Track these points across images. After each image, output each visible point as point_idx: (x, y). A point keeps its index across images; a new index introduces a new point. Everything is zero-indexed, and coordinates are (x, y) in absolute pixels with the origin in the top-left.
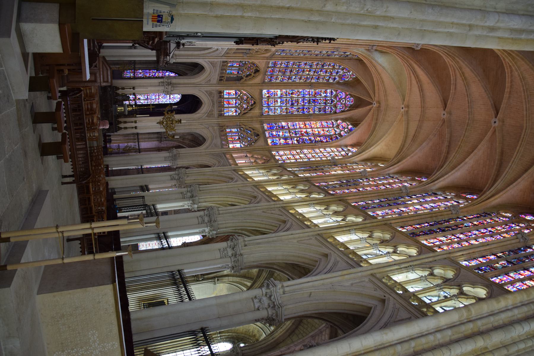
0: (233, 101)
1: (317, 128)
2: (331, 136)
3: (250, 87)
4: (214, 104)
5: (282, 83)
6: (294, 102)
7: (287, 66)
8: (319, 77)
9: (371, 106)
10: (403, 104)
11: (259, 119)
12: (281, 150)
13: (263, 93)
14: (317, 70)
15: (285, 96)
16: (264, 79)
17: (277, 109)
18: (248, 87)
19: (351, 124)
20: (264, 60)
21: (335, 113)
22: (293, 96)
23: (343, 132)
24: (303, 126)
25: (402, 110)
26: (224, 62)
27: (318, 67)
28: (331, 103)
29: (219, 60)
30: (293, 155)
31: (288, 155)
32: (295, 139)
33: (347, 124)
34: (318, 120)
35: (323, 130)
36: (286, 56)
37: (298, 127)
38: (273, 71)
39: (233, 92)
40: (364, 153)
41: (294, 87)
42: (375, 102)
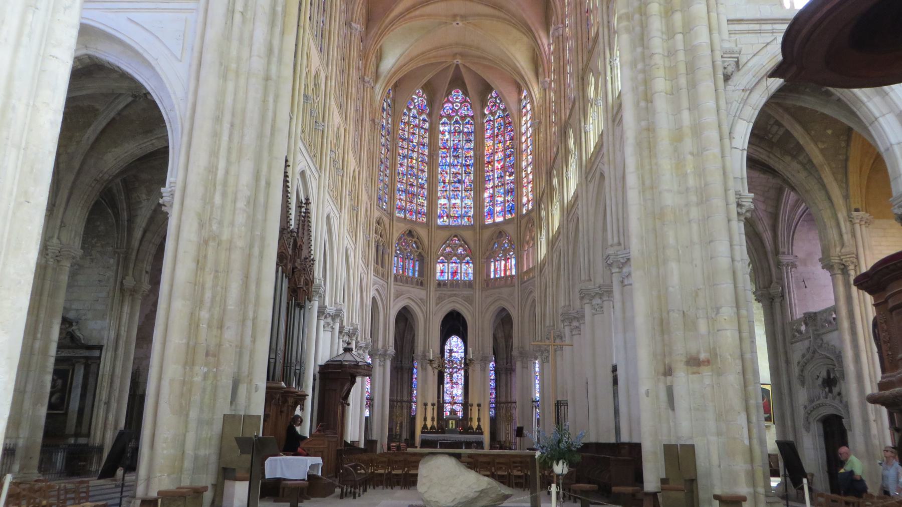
0: (452, 267)
2: (505, 124)
3: (433, 243)
7: (405, 191)
8: (421, 144)
9: (461, 66)
11: (478, 230)
12: (521, 200)
15: (448, 192)
16: (422, 223)
17: (466, 204)
18: (433, 246)
19: (491, 92)
20: (394, 226)
21: (472, 117)
22: (447, 181)
23: (501, 106)
24: (490, 166)
25: (461, 24)
26: (396, 279)
27: (406, 147)
28: (460, 124)
33: (490, 98)
34: (483, 143)
35: (497, 136)
37: (491, 174)
38: (411, 211)
39: (439, 267)
40: (526, 78)
41: (434, 180)
42: (455, 61)
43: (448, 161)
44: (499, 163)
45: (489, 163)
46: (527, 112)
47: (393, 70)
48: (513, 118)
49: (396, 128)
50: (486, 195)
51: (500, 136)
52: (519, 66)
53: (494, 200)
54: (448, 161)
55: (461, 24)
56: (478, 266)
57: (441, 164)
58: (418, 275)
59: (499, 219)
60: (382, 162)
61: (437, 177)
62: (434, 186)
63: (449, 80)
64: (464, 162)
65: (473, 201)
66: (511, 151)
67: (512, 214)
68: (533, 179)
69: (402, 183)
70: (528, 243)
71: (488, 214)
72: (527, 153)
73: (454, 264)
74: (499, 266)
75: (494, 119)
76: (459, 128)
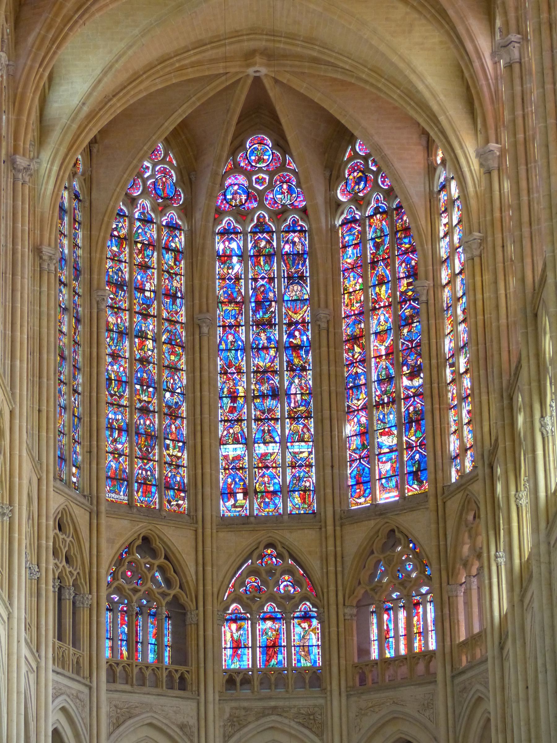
0: (264, 632)
3: (209, 568)
4: (275, 708)
5: (191, 442)
6: (265, 388)
8: (167, 295)
9: (268, 84)
11: (330, 528)
12: (444, 445)
13: (235, 512)
14: (137, 308)
20: (103, 529)
24: (357, 349)
27: (125, 305)
29: (104, 696)
33: (350, 159)
34: (336, 283)
35: (374, 264)
36: (87, 443)
38: (144, 484)
40: (442, 118)
41: (206, 393)
42: (251, 71)
44: (383, 341)
45: (355, 339)
46: (452, 202)
47: (86, 109)
48: (414, 216)
49: (96, 256)
50: (350, 429)
52: (421, 87)
53: (372, 443)
54: (244, 339)
56: (334, 629)
57: (223, 346)
58: (175, 660)
60: (63, 357)
61: (212, 382)
62: (206, 408)
64: (285, 337)
65: (315, 446)
66: (413, 308)
67: (420, 483)
68: (472, 389)
69: (120, 406)
70: (466, 564)
71: (358, 483)
72: (456, 316)
73: (269, 624)
74: (391, 626)
76: (268, 242)
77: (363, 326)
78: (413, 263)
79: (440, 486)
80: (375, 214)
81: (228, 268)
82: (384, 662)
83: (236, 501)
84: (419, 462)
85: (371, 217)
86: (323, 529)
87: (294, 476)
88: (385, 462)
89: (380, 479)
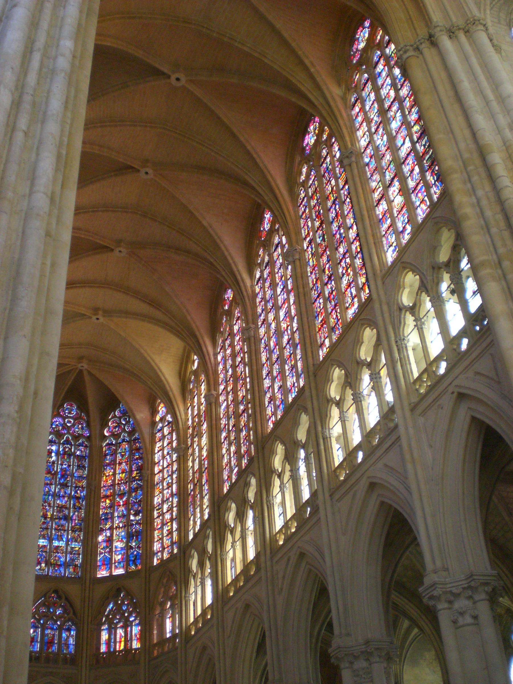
1: (114, 474)
2: (131, 451)
9: (85, 373)
10: (90, 318)
12: (152, 546)
15: (49, 531)
17: (72, 548)
28: (71, 445)
30: (163, 524)
31: (163, 534)
32: (132, 518)
33: (112, 418)
35: (120, 464)
42: (80, 365)
43: (53, 490)
44: (121, 498)
50: (100, 538)
51: (124, 464)
53: (112, 545)
54: (53, 490)
55: (102, 320)
59: (120, 571)
63: (66, 389)
67: (136, 566)
72: (163, 486)
75: (116, 443)
77: (112, 491)
78: (140, 464)
79: (148, 566)
80: (123, 442)
81: (50, 458)
82: (111, 654)
83: (41, 567)
84: (136, 556)
85: (120, 443)
86: (84, 585)
87: (71, 559)
88: (118, 555)
89: (115, 563)
